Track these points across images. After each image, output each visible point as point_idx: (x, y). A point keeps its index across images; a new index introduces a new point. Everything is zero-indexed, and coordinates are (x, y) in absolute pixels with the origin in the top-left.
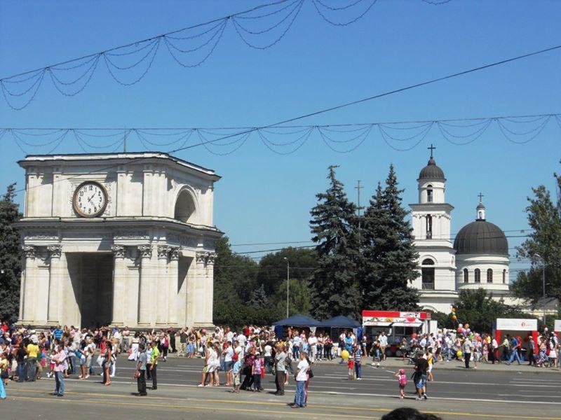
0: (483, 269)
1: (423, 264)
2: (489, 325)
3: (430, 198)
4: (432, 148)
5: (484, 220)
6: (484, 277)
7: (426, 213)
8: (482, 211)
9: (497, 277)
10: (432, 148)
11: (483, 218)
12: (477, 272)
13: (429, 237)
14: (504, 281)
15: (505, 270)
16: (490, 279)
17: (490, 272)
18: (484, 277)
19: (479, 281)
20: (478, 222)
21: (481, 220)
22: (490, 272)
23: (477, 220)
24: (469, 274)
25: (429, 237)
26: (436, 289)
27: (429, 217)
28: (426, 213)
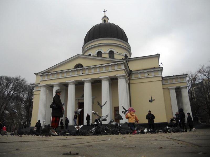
0: (105, 51)
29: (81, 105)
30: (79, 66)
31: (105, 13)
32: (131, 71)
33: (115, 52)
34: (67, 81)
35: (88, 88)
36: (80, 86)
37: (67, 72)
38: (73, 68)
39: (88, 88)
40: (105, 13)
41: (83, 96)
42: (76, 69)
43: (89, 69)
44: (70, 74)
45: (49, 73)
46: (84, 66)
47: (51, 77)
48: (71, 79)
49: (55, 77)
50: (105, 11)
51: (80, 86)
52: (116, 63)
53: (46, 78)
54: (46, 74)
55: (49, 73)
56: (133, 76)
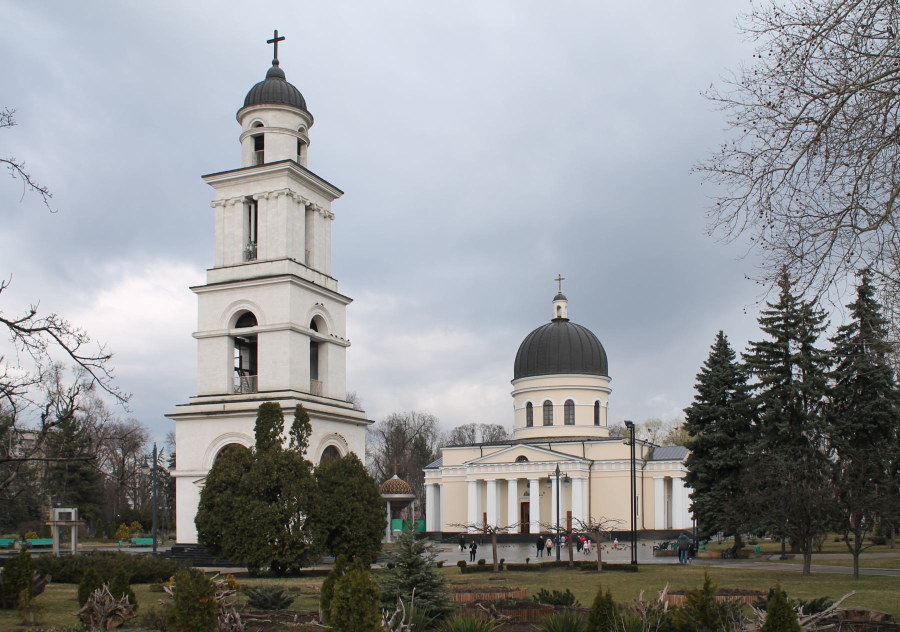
6: (558, 414)
7: (241, 192)
8: (561, 303)
9: (583, 415)
12: (548, 405)
13: (251, 255)
14: (597, 422)
15: (597, 404)
16: (569, 420)
17: (569, 405)
18: (558, 414)
21: (559, 320)
22: (569, 405)
23: (553, 320)
24: (534, 410)
26: (259, 389)
28: (241, 192)
29: (525, 508)
30: (522, 459)
31: (560, 283)
32: (593, 461)
33: (576, 403)
35: (534, 488)
36: (524, 483)
37: (506, 464)
39: (534, 488)
40: (560, 283)
41: (527, 494)
42: (517, 464)
43: (536, 463)
44: (511, 469)
47: (483, 470)
49: (490, 470)
50: (560, 280)
51: (524, 483)
52: (571, 462)
53: (476, 470)
56: (596, 467)
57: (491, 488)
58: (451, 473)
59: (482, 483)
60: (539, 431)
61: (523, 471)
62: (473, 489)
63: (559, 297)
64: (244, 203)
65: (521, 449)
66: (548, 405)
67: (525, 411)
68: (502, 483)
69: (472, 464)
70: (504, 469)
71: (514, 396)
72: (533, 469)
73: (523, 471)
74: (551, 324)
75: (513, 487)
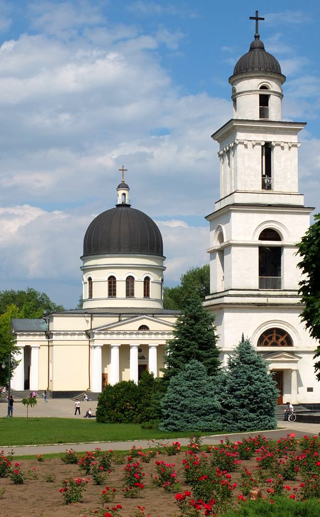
0: (139, 276)
1: (261, 238)
2: (140, 360)
3: (263, 112)
4: (257, 19)
5: (129, 206)
6: (139, 289)
10: (257, 19)
11: (127, 202)
12: (130, 280)
16: (146, 294)
17: (147, 279)
18: (139, 289)
19: (133, 294)
20: (120, 208)
21: (124, 205)
22: (147, 280)
23: (118, 206)
24: (118, 284)
25: (267, 186)
27: (267, 149)
31: (123, 172)
34: (131, 343)
36: (143, 350)
38: (137, 329)
40: (123, 172)
44: (134, 337)
45: (109, 332)
46: (150, 330)
47: (108, 336)
48: (135, 341)
49: (115, 336)
51: (143, 350)
53: (102, 336)
54: (103, 332)
55: (109, 332)
57: (115, 353)
58: (61, 337)
59: (106, 349)
60: (121, 302)
61: (143, 339)
62: (97, 354)
63: (123, 186)
64: (262, 146)
65: (145, 320)
66: (130, 280)
67: (107, 284)
68: (125, 350)
69: (100, 330)
70: (127, 337)
71: (82, 270)
72: (153, 337)
73: (143, 339)
74: (114, 209)
75: (134, 354)
